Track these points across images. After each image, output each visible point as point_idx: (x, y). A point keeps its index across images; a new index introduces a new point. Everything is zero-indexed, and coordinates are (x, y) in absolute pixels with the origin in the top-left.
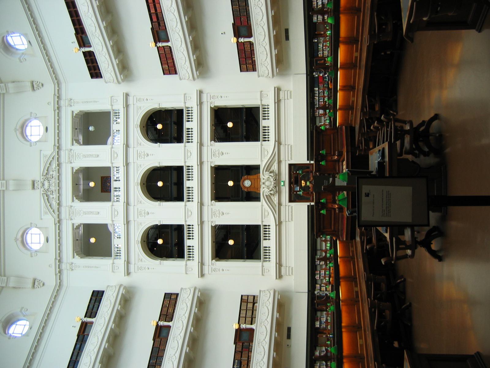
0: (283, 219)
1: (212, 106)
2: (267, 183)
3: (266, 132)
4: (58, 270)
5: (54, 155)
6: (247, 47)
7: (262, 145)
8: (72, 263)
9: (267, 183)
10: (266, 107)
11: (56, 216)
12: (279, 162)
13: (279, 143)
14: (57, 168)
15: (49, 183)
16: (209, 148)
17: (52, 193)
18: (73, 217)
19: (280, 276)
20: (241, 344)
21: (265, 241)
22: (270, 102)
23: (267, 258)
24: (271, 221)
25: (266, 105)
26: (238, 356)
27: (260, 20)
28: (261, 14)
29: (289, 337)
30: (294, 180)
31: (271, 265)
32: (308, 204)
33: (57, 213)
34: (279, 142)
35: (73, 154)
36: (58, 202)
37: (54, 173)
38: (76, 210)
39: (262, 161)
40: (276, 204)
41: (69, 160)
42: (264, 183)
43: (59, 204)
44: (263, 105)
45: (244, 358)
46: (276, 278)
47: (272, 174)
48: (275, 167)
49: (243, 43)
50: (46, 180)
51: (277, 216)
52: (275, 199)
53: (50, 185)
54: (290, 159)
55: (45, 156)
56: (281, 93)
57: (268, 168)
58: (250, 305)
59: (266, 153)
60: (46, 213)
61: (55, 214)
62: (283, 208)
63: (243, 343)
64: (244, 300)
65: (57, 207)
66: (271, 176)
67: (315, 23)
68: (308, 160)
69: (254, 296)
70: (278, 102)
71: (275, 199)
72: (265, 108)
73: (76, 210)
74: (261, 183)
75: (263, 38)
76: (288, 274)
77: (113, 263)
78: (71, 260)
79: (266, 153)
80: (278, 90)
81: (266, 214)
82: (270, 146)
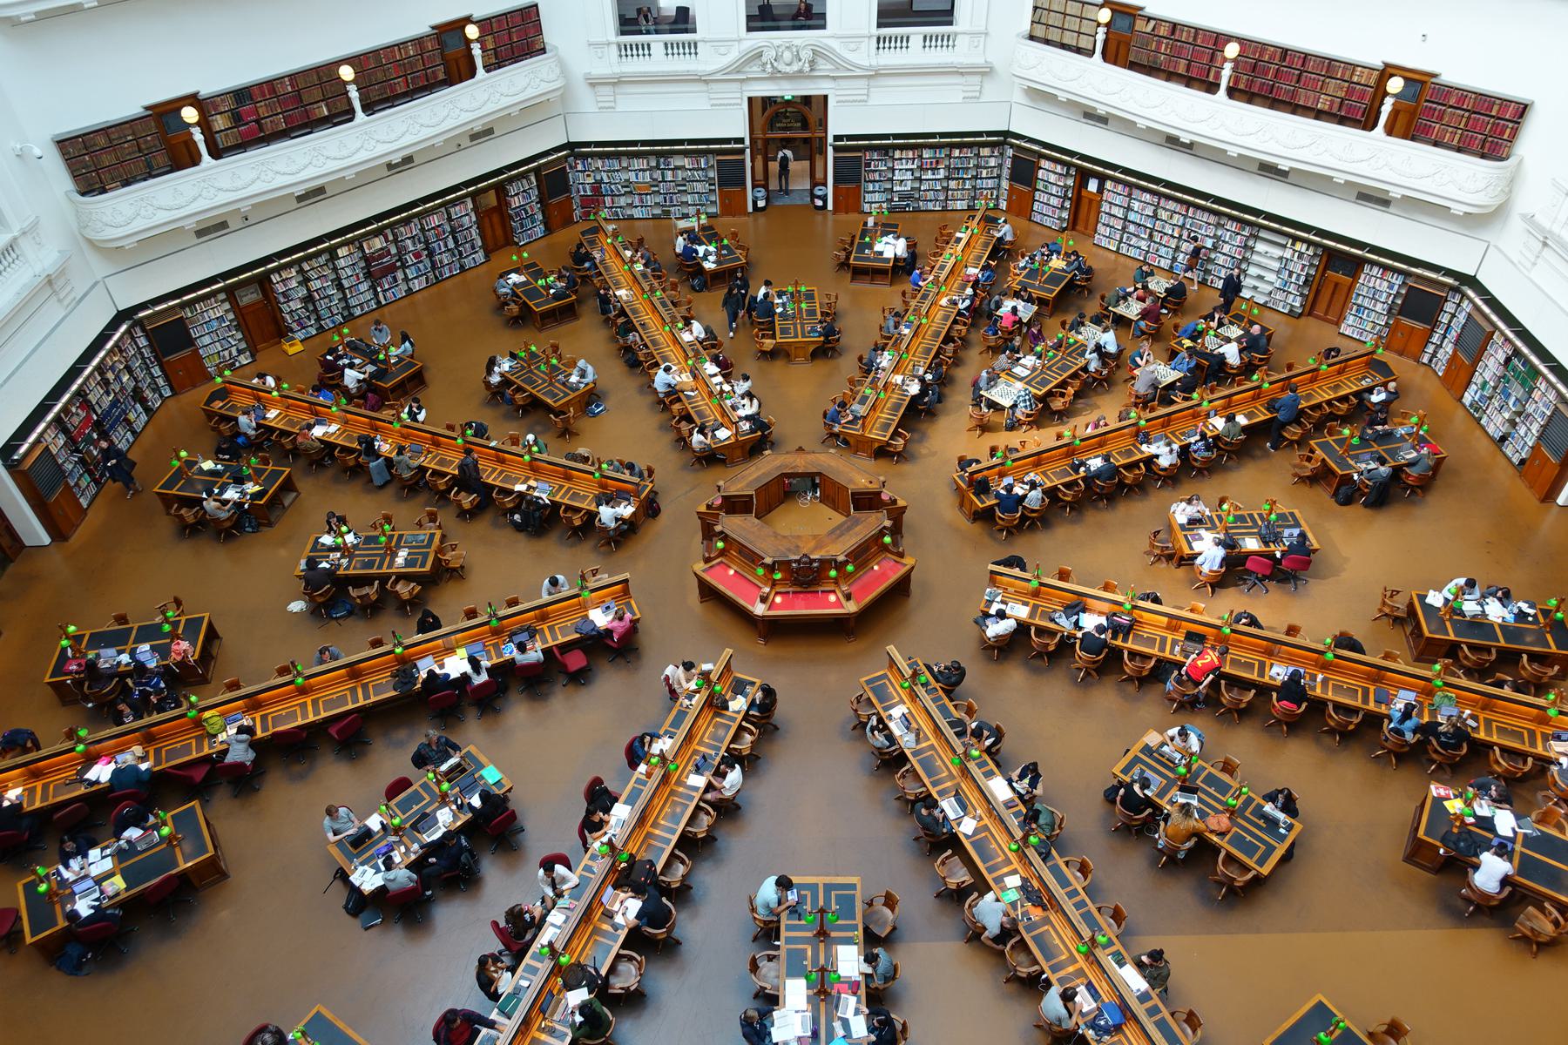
0: (714, 86)
3: (902, 42)
10: (951, 43)
12: (834, 78)
19: (594, 83)
22: (962, 53)
23: (625, 50)
24: (708, 61)
25: (954, 41)
31: (610, 64)
32: (747, 142)
34: (876, 74)
44: (956, 34)
47: (807, 68)
52: (755, 69)
56: (977, 79)
59: (852, 46)
62: (735, 86)
66: (803, 65)
68: (837, 138)
71: (754, 70)
72: (948, 40)
76: (599, 99)
79: (852, 46)
80: (986, 72)
81: (723, 50)
82: (866, 55)
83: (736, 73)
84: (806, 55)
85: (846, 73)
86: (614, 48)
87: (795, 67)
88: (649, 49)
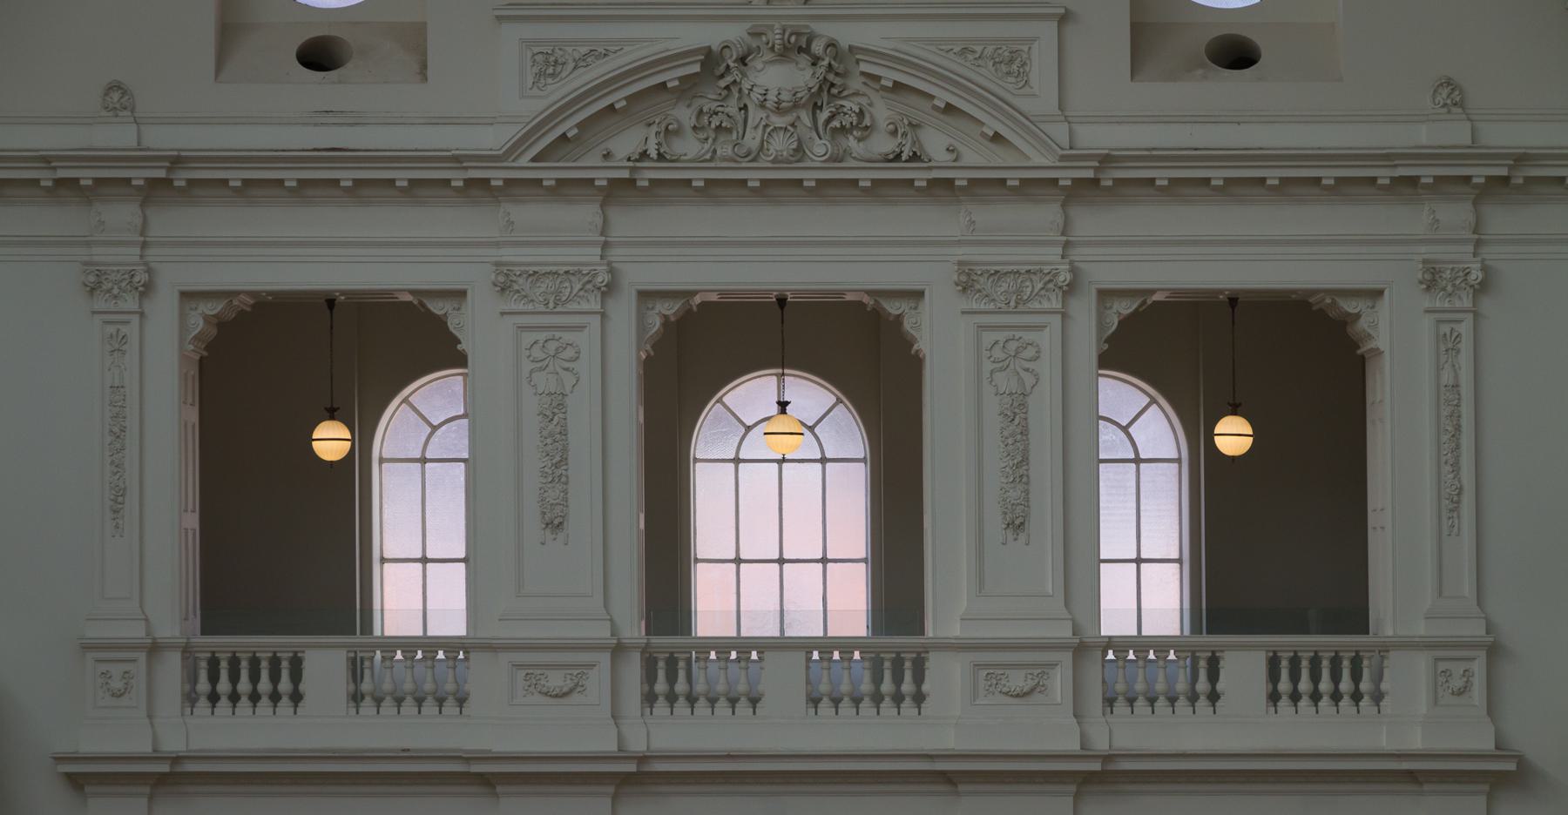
4: (86, 175)
5: (1028, 158)
8: (146, 290)
11: (523, 165)
14: (920, 177)
15: (796, 105)
17: (715, 122)
18: (521, 307)
33: (549, 176)
35: (1035, 305)
36: (645, 177)
37: (882, 144)
38: (581, 328)
41: (978, 270)
43: (620, 190)
50: (821, 70)
53: (779, 110)
55: (1013, 62)
60: (549, 65)
61: (534, 160)
65: (601, 177)
73: (581, 328)
77: (154, 649)
78: (175, 276)
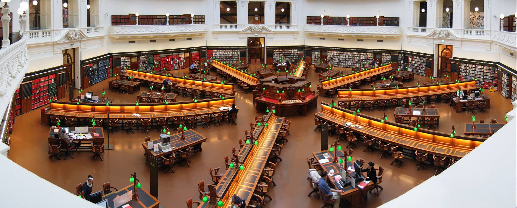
1: (292, 3)
2: (257, 28)
6: (319, 21)
7: (274, 25)
9: (257, 28)
12: (266, 33)
13: (274, 33)
16: (273, 1)
19: (214, 33)
20: (184, 18)
21: (229, 26)
26: (179, 17)
27: (331, 29)
28: (333, 30)
29: (188, 39)
30: (257, 39)
31: (219, 29)
32: (247, 47)
34: (275, 33)
39: (267, 25)
40: (247, 31)
42: (257, 26)
45: (178, 20)
46: (212, 32)
47: (261, 30)
48: (264, 31)
49: (321, 20)
51: (242, 32)
52: (249, 31)
54: (267, 38)
57: (263, 28)
58: (200, 20)
63: (184, 19)
64: (203, 17)
67: (327, 51)
68: (267, 46)
69: (204, 21)
70: (293, 33)
74: (257, 25)
75: (322, 29)
80: (297, 33)
81: (243, 27)
82: (273, 29)
83: (244, 32)
84: (261, 28)
85: (269, 32)
86: (219, 26)
87: (258, 30)
88: (227, 27)
